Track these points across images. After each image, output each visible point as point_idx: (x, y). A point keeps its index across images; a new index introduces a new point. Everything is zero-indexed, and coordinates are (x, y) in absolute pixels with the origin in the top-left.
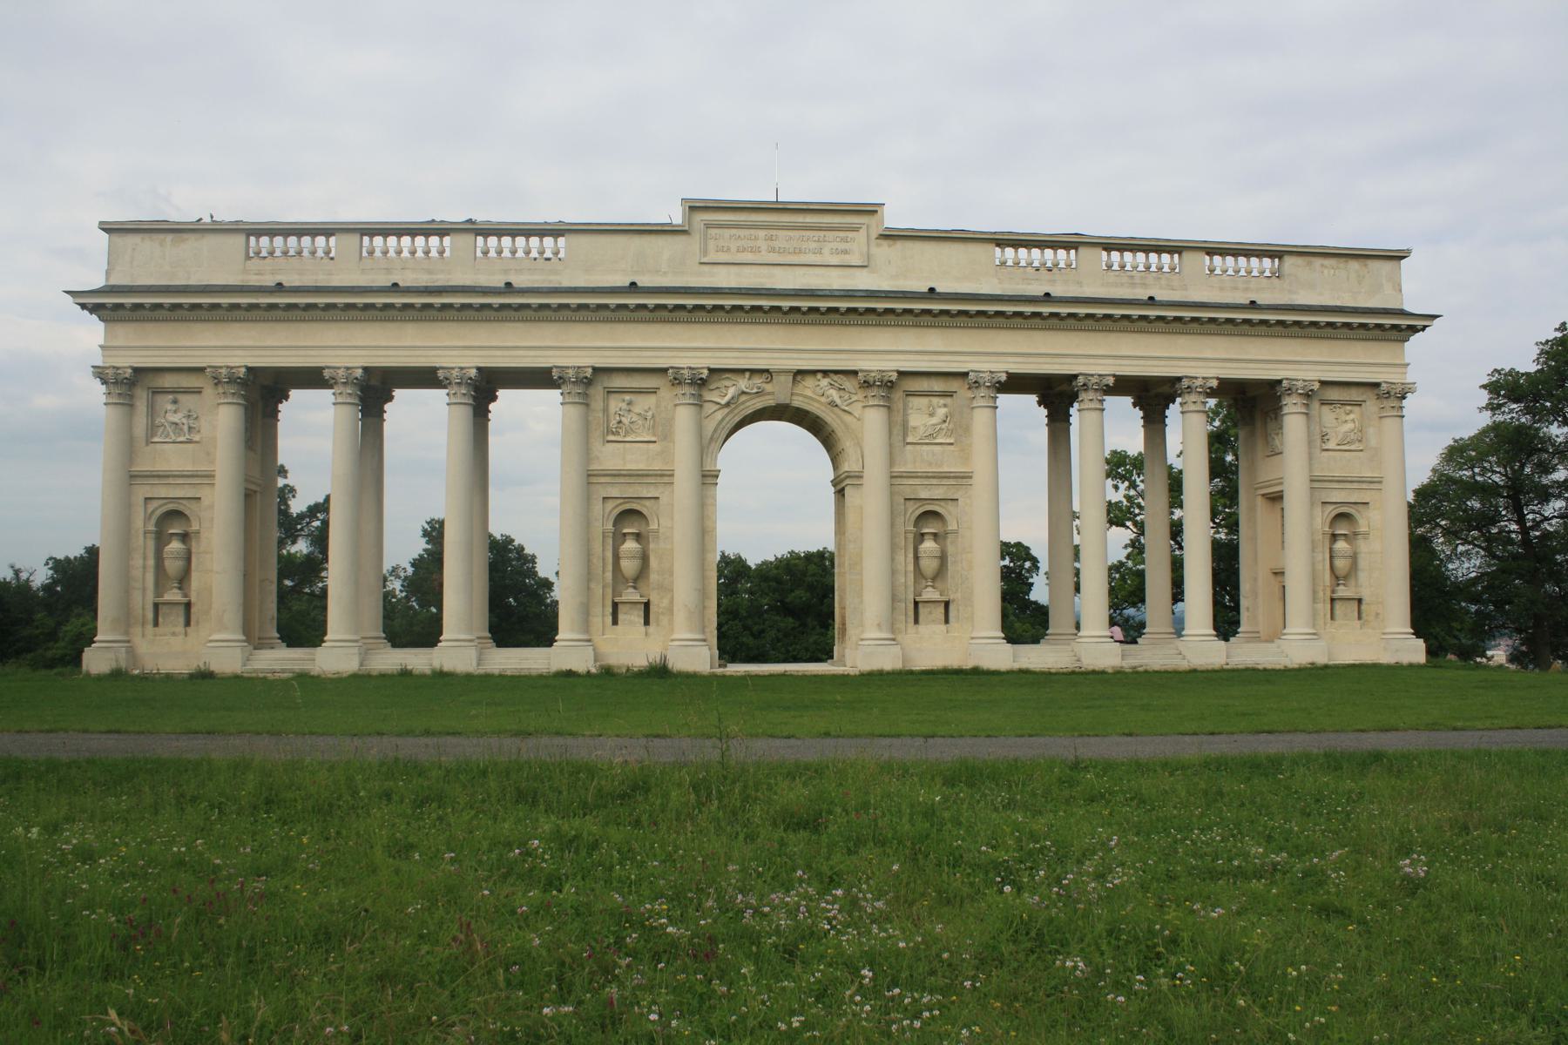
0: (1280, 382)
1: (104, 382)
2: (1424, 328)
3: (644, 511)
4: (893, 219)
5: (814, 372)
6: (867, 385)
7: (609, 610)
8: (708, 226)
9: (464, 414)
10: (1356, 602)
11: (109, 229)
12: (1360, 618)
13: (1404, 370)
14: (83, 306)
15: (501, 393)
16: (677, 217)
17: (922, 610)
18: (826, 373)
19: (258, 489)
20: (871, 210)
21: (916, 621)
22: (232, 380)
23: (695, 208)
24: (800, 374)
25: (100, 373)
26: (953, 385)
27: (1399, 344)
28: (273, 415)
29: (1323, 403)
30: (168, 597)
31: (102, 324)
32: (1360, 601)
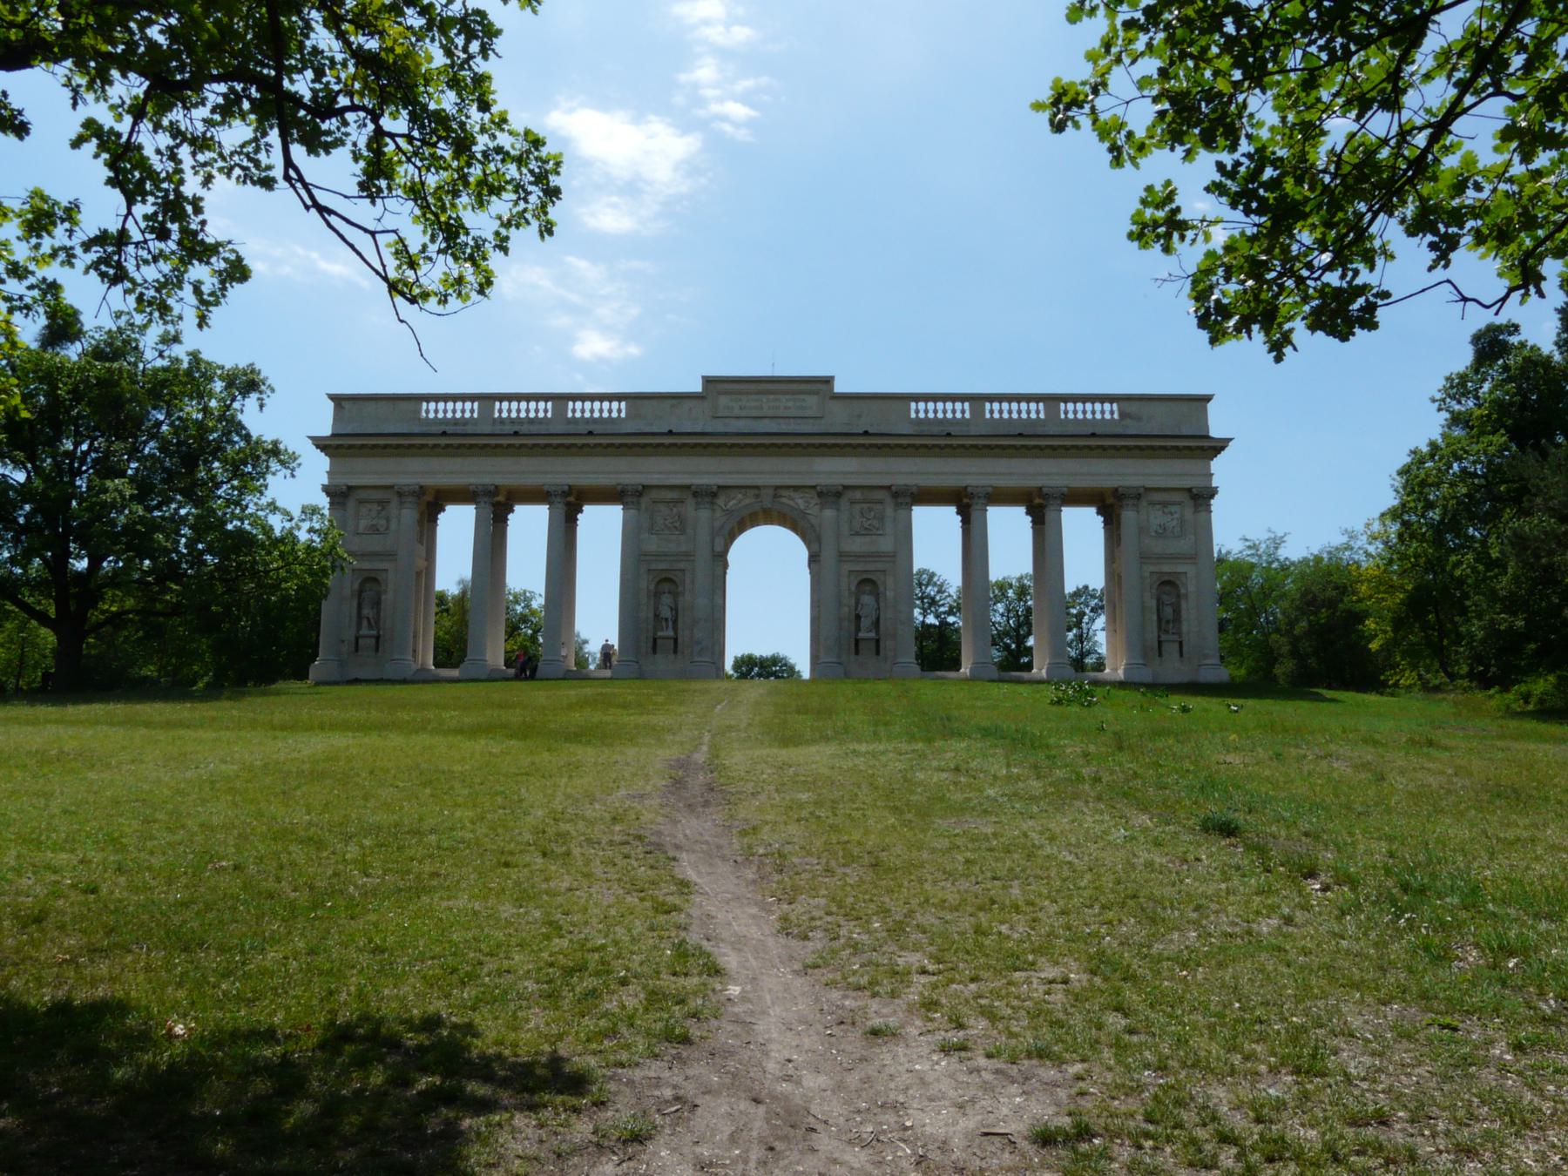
2: (1223, 448)
5: (788, 487)
7: (650, 645)
8: (719, 393)
11: (333, 397)
12: (1181, 655)
14: (318, 447)
16: (697, 387)
17: (861, 645)
18: (796, 488)
20: (828, 381)
21: (857, 653)
22: (413, 493)
23: (708, 381)
24: (777, 488)
26: (880, 495)
29: (1152, 504)
30: (364, 631)
32: (1181, 644)
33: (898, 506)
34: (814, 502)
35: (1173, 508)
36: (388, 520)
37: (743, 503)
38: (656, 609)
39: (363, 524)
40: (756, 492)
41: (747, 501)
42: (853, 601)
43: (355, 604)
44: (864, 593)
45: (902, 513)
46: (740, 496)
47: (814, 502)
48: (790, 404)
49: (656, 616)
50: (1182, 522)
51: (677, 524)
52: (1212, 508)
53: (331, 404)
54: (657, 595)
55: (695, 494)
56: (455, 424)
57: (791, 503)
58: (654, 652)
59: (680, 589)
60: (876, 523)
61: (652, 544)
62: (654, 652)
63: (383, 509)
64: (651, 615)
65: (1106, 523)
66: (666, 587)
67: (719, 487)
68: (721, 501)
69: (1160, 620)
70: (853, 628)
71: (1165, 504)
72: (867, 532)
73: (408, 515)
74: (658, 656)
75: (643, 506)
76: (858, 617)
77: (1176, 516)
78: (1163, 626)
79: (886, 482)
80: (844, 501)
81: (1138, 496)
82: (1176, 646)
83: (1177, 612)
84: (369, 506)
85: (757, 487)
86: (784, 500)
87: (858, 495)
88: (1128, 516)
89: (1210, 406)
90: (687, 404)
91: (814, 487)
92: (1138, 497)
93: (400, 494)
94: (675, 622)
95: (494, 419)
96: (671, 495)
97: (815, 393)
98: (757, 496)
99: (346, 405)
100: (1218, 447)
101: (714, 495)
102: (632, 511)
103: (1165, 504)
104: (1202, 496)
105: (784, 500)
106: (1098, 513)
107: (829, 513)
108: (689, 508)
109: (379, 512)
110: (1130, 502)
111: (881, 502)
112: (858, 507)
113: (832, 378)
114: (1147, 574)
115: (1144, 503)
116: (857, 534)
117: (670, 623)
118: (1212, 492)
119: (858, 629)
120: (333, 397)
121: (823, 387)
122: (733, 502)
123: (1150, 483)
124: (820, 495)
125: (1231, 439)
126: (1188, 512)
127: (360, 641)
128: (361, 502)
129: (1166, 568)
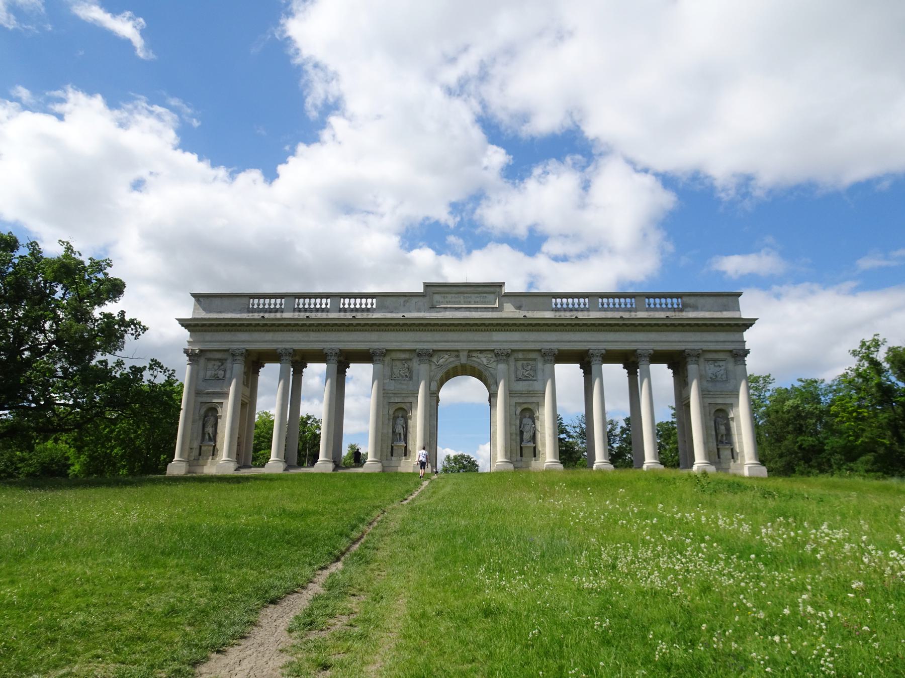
0: (684, 351)
1: (188, 355)
2: (751, 325)
3: (405, 408)
4: (507, 289)
6: (497, 355)
7: (389, 450)
9: (334, 366)
10: (730, 451)
11: (195, 295)
13: (743, 344)
15: (351, 365)
16: (420, 289)
17: (525, 451)
18: (481, 351)
19: (248, 402)
20: (501, 285)
23: (427, 286)
24: (470, 351)
25: (186, 351)
27: (741, 333)
28: (256, 373)
29: (708, 360)
31: (189, 333)
33: (545, 362)
34: (492, 360)
35: (721, 363)
36: (225, 371)
37: (448, 361)
38: (394, 427)
39: (209, 373)
41: (452, 359)
42: (518, 422)
43: (201, 423)
44: (525, 417)
45: (548, 366)
46: (447, 356)
47: (492, 360)
48: (478, 299)
49: (394, 432)
50: (727, 371)
52: (746, 363)
53: (193, 299)
54: (395, 418)
55: (419, 355)
56: (270, 312)
57: (478, 360)
58: (392, 455)
60: (532, 373)
61: (392, 386)
62: (392, 455)
63: (222, 364)
64: (391, 431)
65: (675, 374)
67: (434, 351)
68: (434, 359)
70: (518, 440)
71: (715, 361)
72: (526, 378)
73: (238, 368)
74: (393, 458)
75: (386, 362)
76: (522, 433)
77: (723, 368)
78: (719, 438)
79: (537, 346)
80: (512, 359)
81: (698, 355)
82: (729, 452)
84: (213, 362)
85: (457, 351)
86: (474, 359)
87: (520, 356)
88: (692, 368)
89: (740, 299)
90: (415, 300)
91: (493, 351)
92: (698, 356)
93: (233, 355)
95: (295, 309)
96: (403, 356)
97: (493, 293)
99: (201, 299)
100: (748, 324)
101: (431, 355)
102: (380, 366)
103: (715, 361)
104: (740, 354)
105: (474, 359)
106: (669, 368)
107: (502, 367)
108: (415, 364)
109: (219, 366)
110: (694, 359)
111: (535, 360)
112: (520, 363)
113: (504, 283)
114: (707, 405)
115: (702, 360)
116: (520, 380)
117: (402, 437)
119: (522, 440)
120: (195, 295)
121: (498, 289)
123: (705, 348)
124: (497, 355)
125: (757, 319)
126: (731, 366)
127: (202, 448)
128: (209, 360)
129: (720, 401)
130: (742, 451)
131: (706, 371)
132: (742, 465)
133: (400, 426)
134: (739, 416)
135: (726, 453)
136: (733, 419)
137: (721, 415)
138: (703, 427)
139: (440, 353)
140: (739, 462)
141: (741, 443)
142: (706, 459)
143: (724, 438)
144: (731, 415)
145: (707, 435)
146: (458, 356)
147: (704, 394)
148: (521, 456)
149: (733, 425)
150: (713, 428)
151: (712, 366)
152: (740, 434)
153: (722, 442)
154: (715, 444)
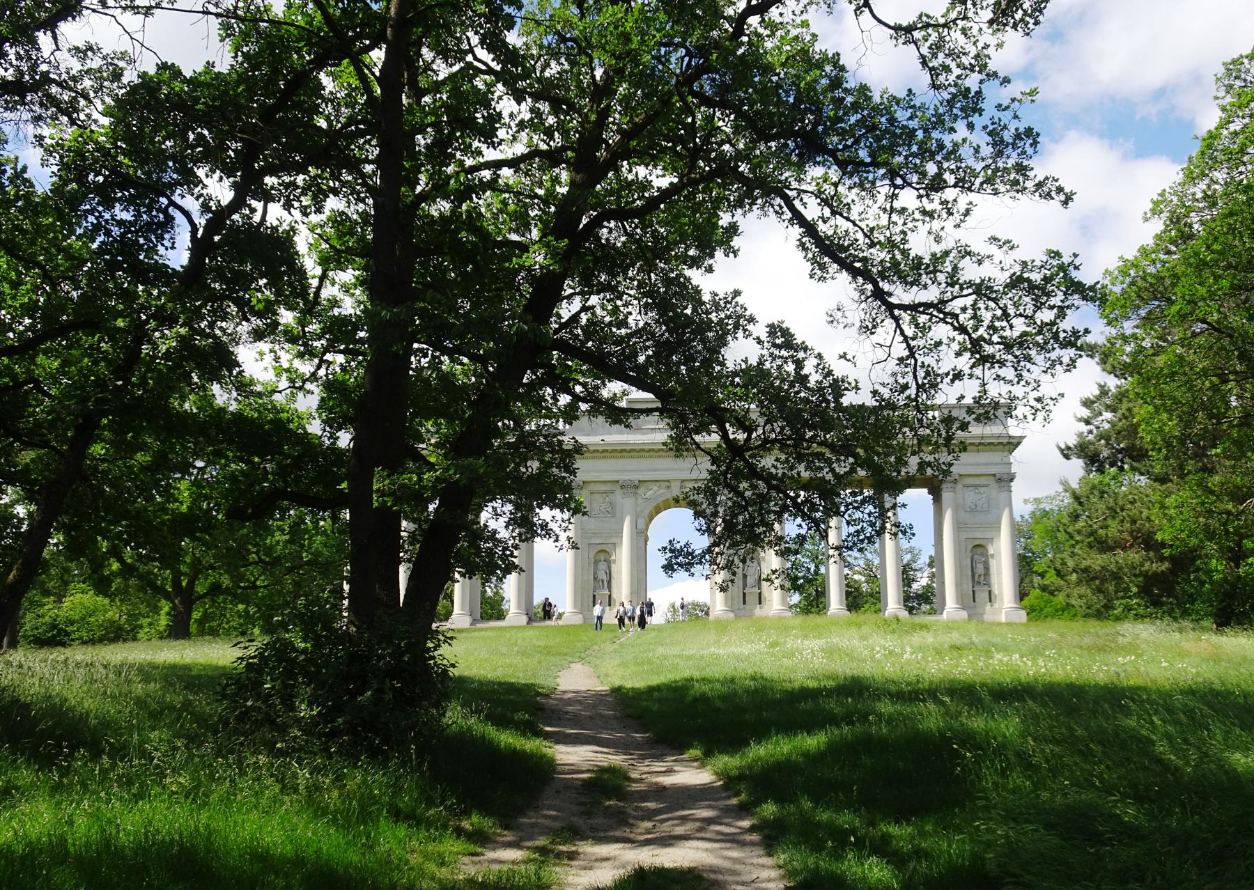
2: (1019, 443)
24: (683, 481)
35: (982, 490)
38: (595, 573)
40: (667, 484)
41: (662, 491)
49: (595, 578)
50: (989, 500)
51: (610, 510)
54: (596, 562)
55: (622, 487)
59: (613, 558)
66: (602, 557)
68: (641, 491)
69: (973, 576)
71: (976, 486)
82: (987, 595)
83: (987, 569)
94: (609, 582)
98: (668, 487)
103: (976, 486)
104: (1005, 480)
108: (618, 497)
110: (949, 485)
115: (959, 486)
118: (1012, 478)
122: (652, 492)
129: (978, 535)
130: (1001, 594)
131: (964, 498)
132: (1001, 609)
133: (602, 572)
134: (1000, 552)
135: (982, 595)
136: (992, 556)
137: (979, 550)
138: (956, 565)
139: (647, 484)
140: (996, 605)
141: (1000, 583)
142: (957, 603)
143: (982, 578)
144: (991, 551)
145: (961, 575)
146: (668, 487)
147: (959, 527)
148: (744, 603)
149: (993, 563)
150: (970, 568)
151: (972, 493)
152: (1000, 573)
153: (979, 583)
154: (971, 585)
